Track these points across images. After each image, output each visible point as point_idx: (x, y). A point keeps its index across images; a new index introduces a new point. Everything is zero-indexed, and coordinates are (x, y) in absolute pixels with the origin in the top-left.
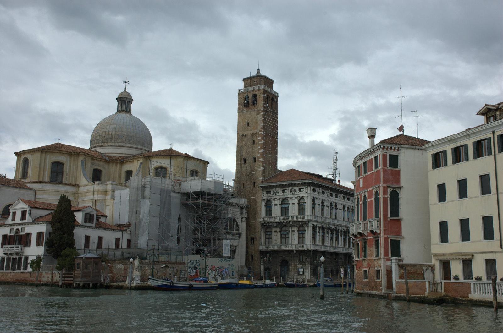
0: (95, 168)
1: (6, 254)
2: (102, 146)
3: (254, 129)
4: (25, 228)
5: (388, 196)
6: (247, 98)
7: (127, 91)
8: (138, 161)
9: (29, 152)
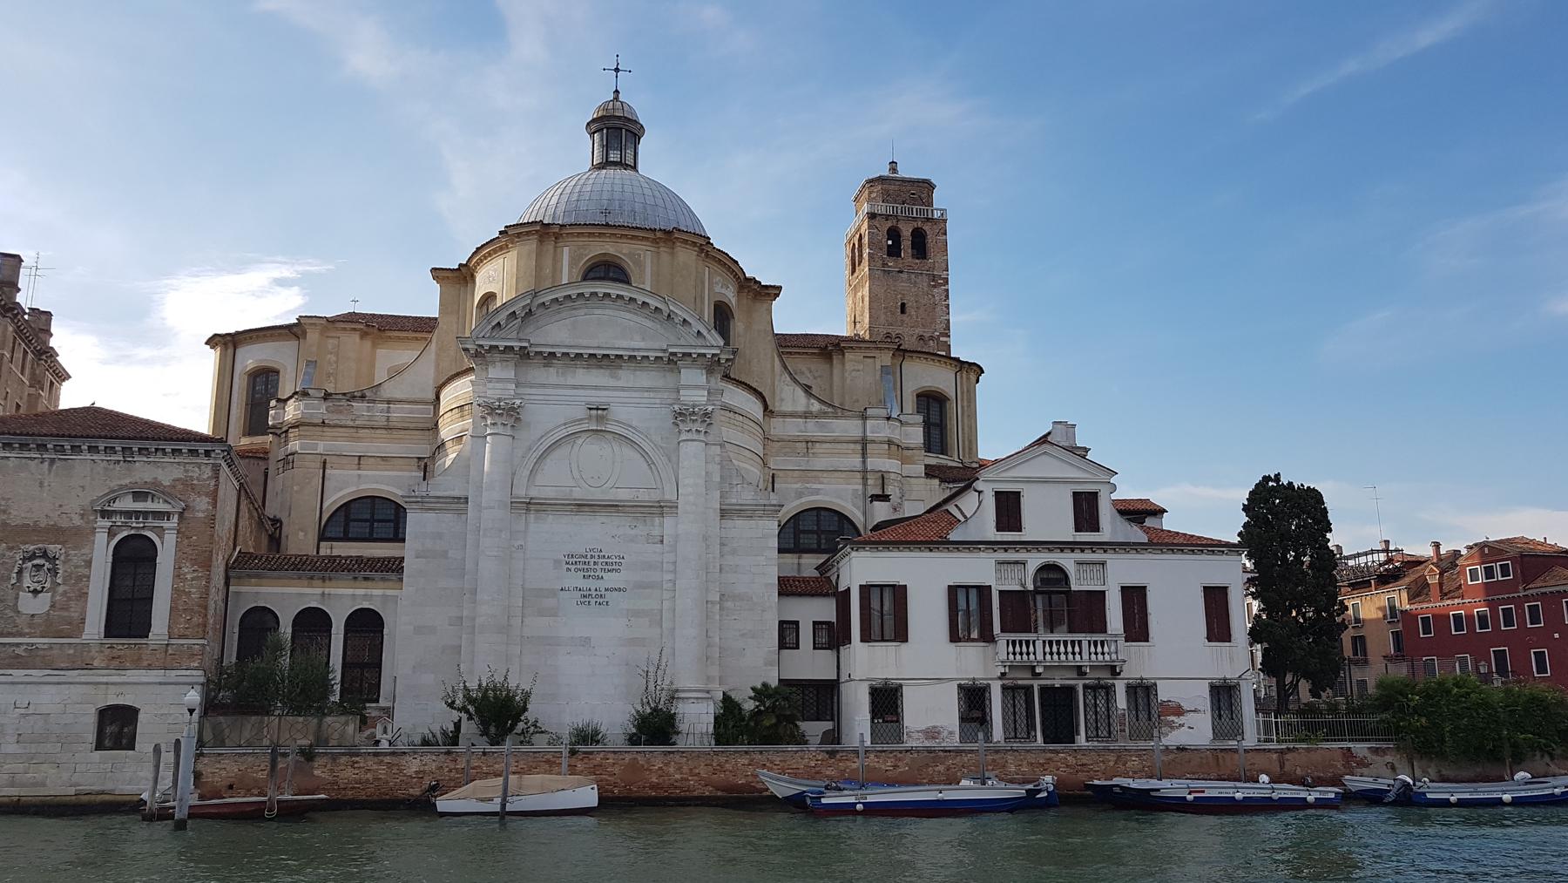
3: (923, 325)
4: (1103, 564)
6: (894, 233)
8: (864, 357)
9: (634, 237)
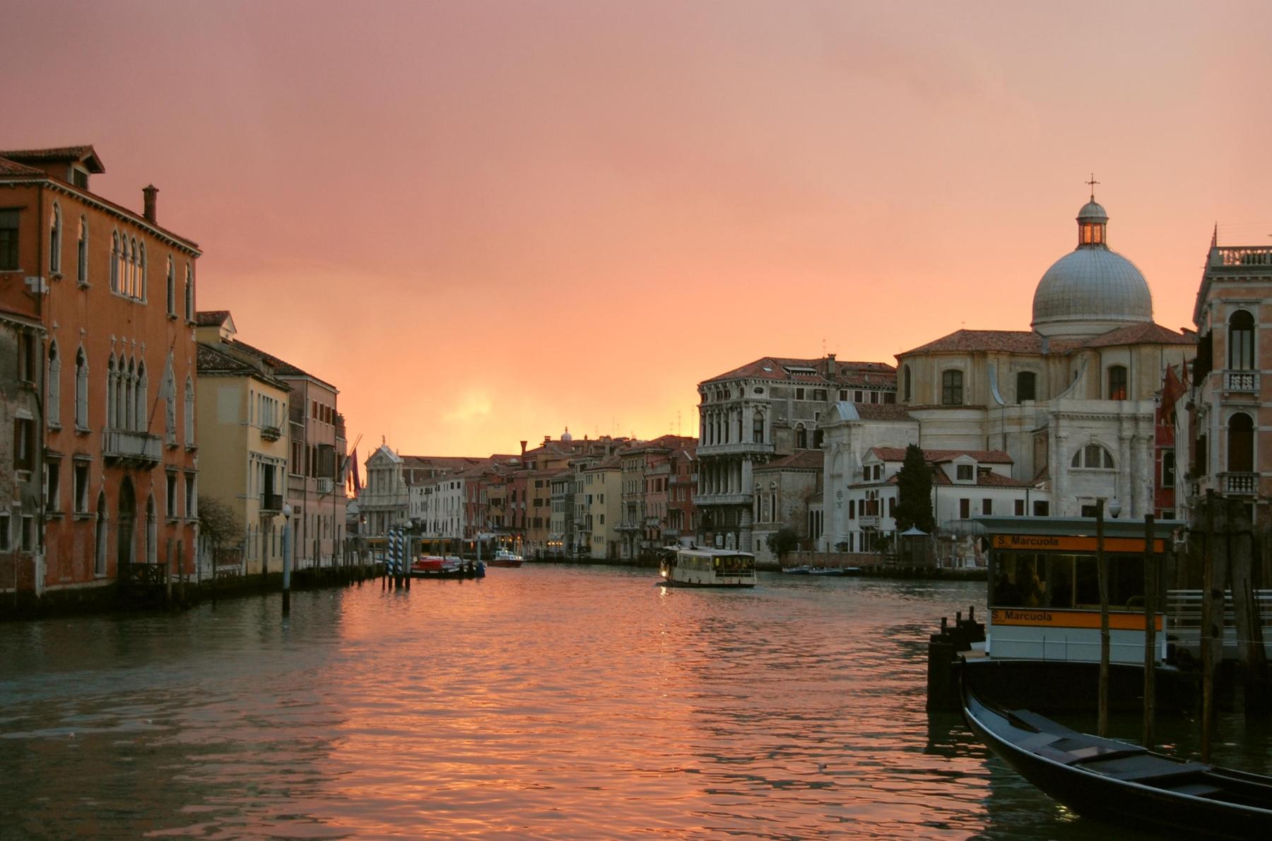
0: (1021, 370)
1: (862, 528)
2: (1044, 323)
5: (1162, 459)
7: (1096, 201)
